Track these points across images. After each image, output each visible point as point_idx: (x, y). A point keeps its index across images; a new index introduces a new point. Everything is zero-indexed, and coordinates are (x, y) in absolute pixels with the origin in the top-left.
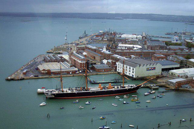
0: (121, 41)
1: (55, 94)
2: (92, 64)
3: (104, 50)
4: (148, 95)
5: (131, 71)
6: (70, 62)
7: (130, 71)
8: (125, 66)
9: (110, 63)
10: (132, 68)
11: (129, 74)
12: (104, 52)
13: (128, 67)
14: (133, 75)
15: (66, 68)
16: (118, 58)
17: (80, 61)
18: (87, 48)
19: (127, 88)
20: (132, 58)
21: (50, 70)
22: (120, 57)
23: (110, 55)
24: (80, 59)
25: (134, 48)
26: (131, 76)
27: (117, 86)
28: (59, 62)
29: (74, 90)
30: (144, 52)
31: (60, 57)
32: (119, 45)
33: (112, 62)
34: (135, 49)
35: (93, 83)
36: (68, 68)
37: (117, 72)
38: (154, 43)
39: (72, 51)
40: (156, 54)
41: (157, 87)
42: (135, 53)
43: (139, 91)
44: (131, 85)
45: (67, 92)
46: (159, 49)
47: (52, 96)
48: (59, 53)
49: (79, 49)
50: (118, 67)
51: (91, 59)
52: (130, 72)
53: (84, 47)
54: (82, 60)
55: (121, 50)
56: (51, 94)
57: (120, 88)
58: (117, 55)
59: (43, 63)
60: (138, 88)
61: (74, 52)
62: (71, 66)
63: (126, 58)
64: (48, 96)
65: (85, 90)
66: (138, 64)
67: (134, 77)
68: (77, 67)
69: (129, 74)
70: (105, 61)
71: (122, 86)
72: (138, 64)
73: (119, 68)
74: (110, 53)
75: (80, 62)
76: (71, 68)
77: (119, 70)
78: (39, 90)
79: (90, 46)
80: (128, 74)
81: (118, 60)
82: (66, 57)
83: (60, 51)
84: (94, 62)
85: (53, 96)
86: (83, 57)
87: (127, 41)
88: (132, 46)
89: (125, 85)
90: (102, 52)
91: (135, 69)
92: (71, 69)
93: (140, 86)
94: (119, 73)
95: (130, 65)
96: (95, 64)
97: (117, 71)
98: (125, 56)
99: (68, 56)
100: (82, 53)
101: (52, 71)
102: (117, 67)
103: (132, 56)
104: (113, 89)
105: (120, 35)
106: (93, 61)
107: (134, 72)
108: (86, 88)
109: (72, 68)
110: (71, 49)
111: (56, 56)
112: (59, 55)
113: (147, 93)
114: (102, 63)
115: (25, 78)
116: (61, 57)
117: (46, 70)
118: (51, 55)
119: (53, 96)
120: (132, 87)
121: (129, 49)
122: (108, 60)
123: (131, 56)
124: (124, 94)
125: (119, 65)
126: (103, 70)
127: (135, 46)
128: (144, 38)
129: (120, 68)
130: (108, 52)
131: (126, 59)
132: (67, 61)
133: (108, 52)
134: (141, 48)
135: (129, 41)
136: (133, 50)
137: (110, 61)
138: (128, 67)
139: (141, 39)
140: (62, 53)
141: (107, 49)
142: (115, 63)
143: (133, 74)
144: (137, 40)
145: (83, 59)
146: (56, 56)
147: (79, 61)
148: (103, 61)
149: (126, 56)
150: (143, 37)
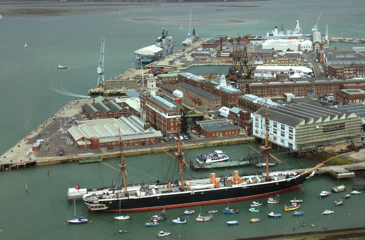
0: (262, 57)
1: (109, 201)
2: (195, 119)
3: (223, 85)
4: (327, 196)
5: (287, 135)
6: (144, 116)
7: (283, 135)
8: (271, 123)
9: (235, 115)
10: (287, 128)
11: (282, 141)
12: (222, 88)
13: (279, 125)
14: (290, 145)
15: (135, 131)
16: (255, 102)
17: (166, 114)
18: (181, 79)
19: (276, 180)
20: (289, 100)
21: (97, 140)
22: (260, 99)
23: (235, 95)
24: (167, 109)
25: (293, 73)
26: (287, 145)
27: (253, 176)
28: (117, 118)
29: (154, 191)
30: (316, 85)
31: (119, 104)
32: (258, 68)
33: (241, 113)
34: (296, 76)
35: (197, 170)
36: (138, 131)
37: (254, 136)
38: (342, 59)
40: (347, 88)
41: (349, 174)
42: (296, 89)
43: (304, 187)
44: (285, 173)
45: (136, 195)
46: (354, 73)
47: (103, 207)
48: (119, 95)
50: (254, 124)
51: (192, 106)
52: (283, 138)
53: (175, 77)
54: (170, 113)
55: (263, 80)
56: (100, 202)
57: (260, 180)
58: (253, 94)
59: (82, 122)
60: (302, 179)
61: (153, 93)
62: (145, 129)
63: (273, 100)
64: (92, 207)
65: (177, 188)
66: (301, 117)
67: (294, 148)
68: (160, 129)
69: (282, 141)
70: (225, 111)
71: (265, 175)
72: (301, 117)
73: (257, 126)
74: (236, 90)
75: (167, 117)
76: (146, 131)
77: (257, 132)
78: (73, 192)
79: (189, 75)
80: (278, 142)
81: (254, 108)
82: (134, 103)
83: (121, 88)
84: (199, 113)
85: (106, 208)
86: (172, 105)
87: (275, 56)
88: (285, 68)
89: (271, 174)
90: (218, 88)
91: (294, 130)
92: (146, 133)
93: (308, 174)
94: (259, 141)
95: (285, 121)
96: (201, 118)
97: (254, 133)
98: (271, 95)
99: (138, 102)
100: (171, 92)
101: (102, 141)
102: (251, 125)
103: (288, 94)
104: (244, 185)
105: (259, 42)
106: (198, 112)
107: (294, 137)
108: (180, 183)
109: (148, 131)
112: (118, 100)
113: (324, 192)
114: (219, 116)
115: (40, 160)
116: (124, 103)
117: (87, 139)
118: (99, 99)
119: (106, 208)
120: (287, 177)
121: (281, 76)
122: (231, 107)
123: (286, 96)
124: (269, 196)
125: (257, 120)
126: (221, 133)
127: (295, 68)
128: (317, 46)
129: (260, 127)
130: (230, 89)
131: (274, 104)
132: (139, 116)
133: (230, 89)
134: (310, 73)
135: (280, 57)
136: (291, 80)
137: (236, 110)
138: (279, 125)
139: (310, 49)
140: (124, 94)
141: (228, 83)
142: (248, 117)
143: (291, 141)
144: (301, 53)
145: (174, 108)
147: (163, 114)
148: (221, 110)
149: (275, 95)
150: (314, 45)
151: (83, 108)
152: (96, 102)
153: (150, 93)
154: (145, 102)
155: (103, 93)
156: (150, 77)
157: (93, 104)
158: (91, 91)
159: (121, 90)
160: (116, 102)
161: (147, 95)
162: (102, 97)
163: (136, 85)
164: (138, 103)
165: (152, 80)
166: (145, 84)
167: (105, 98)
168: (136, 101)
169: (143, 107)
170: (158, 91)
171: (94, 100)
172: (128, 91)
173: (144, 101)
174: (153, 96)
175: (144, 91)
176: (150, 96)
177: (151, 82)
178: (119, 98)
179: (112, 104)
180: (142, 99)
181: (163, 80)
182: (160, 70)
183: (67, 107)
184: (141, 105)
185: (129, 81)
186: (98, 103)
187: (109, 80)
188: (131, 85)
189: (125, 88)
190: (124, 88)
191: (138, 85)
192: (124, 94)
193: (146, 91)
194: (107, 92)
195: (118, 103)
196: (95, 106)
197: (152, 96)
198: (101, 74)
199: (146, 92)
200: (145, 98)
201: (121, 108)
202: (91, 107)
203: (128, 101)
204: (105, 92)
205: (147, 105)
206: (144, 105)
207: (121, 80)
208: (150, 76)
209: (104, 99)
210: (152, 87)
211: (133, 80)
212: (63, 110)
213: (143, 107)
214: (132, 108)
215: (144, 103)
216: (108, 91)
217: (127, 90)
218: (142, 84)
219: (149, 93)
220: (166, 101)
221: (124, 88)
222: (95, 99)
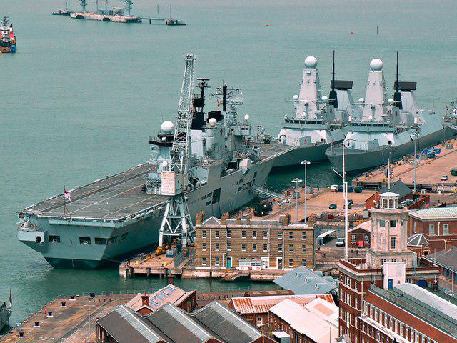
31: (250, 318)
39: (368, 257)
49: (436, 245)
61: (395, 272)
99: (329, 312)
110: (361, 238)
111: (217, 306)
116: (268, 315)
140: (266, 284)
146: (217, 306)
151: (101, 329)
152: (154, 307)
153: (382, 270)
154: (359, 308)
155: (179, 276)
156: (385, 206)
157: (143, 313)
158: (133, 269)
159: (254, 268)
160: (237, 309)
161: (372, 276)
162: (179, 289)
163: (316, 249)
164: (327, 318)
165: (393, 218)
166: (354, 249)
167: (189, 293)
168: (319, 307)
169: (352, 329)
170: (416, 266)
171: (145, 298)
172: (287, 275)
173: (354, 306)
174: (395, 285)
175: (358, 262)
176: (380, 285)
177: (387, 224)
178: (247, 295)
179: (219, 317)
180: (348, 297)
181: (432, 234)
182: (414, 197)
183: (37, 324)
184: (342, 323)
185: (291, 231)
186: (161, 311)
187: (207, 226)
188: (298, 246)
189: (272, 259)
190: (267, 259)
191: (324, 249)
192: (266, 284)
193: (364, 261)
194: (196, 274)
195: (244, 316)
196: (148, 322)
197: (390, 281)
198: (173, 199)
199: (365, 266)
200: (359, 290)
201: (256, 334)
202: (134, 324)
203: (284, 308)
204: (186, 274)
205: (369, 320)
206: (353, 323)
207: (254, 226)
208: (385, 201)
209: (184, 298)
210: (393, 246)
211: (305, 226)
212: (22, 335)
213: (352, 329)
214: (303, 335)
215: (355, 314)
216: (201, 271)
217: (280, 267)
218: (340, 249)
219: (377, 271)
220: (449, 303)
221: (267, 259)
222: (151, 296)
